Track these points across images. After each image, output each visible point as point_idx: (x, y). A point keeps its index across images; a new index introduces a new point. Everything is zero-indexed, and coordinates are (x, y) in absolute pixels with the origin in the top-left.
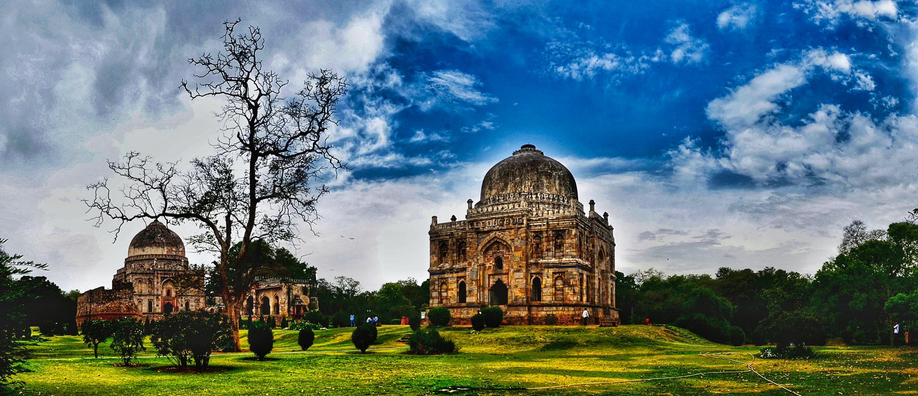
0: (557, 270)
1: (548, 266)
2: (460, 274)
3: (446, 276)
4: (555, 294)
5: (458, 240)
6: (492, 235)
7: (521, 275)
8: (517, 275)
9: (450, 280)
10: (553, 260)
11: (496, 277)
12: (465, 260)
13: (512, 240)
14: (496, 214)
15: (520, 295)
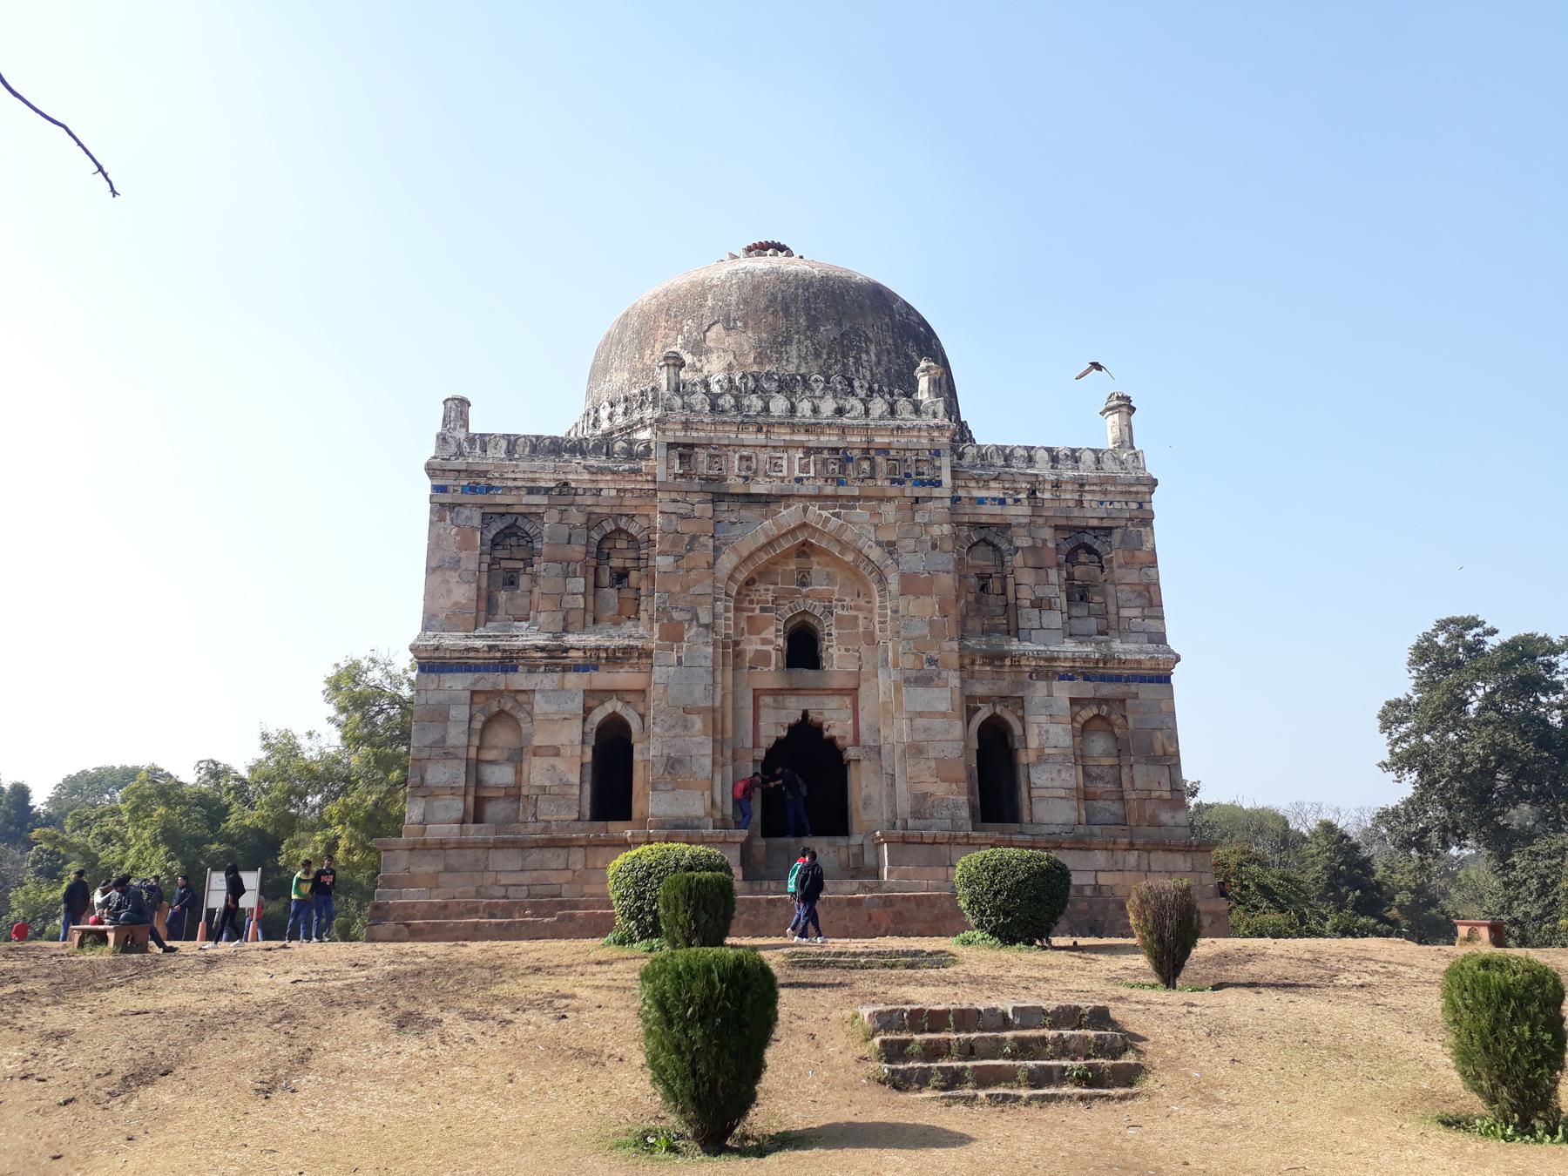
0: (1087, 689)
1: (1048, 670)
3: (520, 680)
5: (593, 521)
6: (789, 515)
9: (541, 705)
10: (1070, 647)
13: (890, 547)
15: (939, 789)
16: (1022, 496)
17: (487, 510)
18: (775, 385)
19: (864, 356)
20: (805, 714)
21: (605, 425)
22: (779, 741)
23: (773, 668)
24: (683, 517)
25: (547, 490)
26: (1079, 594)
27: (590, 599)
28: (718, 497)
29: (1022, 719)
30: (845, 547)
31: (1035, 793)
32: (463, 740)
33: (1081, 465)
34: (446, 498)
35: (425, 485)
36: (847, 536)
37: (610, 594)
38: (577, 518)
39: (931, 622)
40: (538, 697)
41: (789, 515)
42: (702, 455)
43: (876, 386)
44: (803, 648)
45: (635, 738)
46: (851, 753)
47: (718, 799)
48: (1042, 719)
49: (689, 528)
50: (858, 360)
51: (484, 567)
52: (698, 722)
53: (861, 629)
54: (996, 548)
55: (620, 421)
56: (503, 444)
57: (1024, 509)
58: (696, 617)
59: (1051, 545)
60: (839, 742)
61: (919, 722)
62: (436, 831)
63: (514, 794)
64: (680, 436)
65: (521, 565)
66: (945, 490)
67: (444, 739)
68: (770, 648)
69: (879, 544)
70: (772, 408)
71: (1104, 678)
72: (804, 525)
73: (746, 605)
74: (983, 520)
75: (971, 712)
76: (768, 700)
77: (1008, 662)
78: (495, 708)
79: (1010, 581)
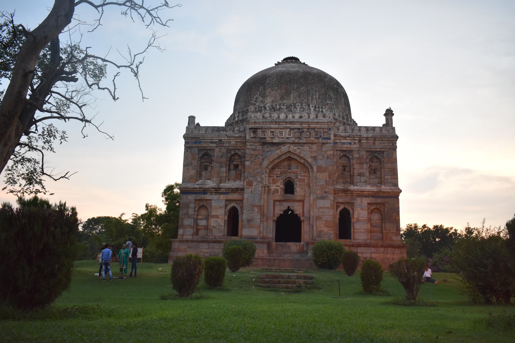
1: (362, 194)
2: (231, 196)
3: (208, 197)
4: (371, 232)
5: (228, 151)
6: (284, 149)
7: (327, 203)
8: (321, 203)
9: (214, 204)
10: (369, 188)
12: (238, 177)
14: (291, 123)
15: (326, 229)
16: (357, 142)
17: (200, 148)
18: (285, 107)
19: (314, 97)
20: (289, 207)
21: (236, 119)
22: (281, 215)
23: (279, 194)
24: (254, 150)
25: (216, 142)
26: (373, 171)
27: (227, 174)
28: (264, 144)
29: (353, 209)
30: (301, 158)
31: (355, 231)
32: (193, 213)
33: (375, 132)
34: (188, 145)
35: (183, 141)
36: (301, 155)
37: (233, 172)
38: (224, 150)
39: (326, 181)
40: (213, 201)
41: (284, 149)
42: (259, 132)
43: (317, 106)
44: (289, 187)
45: (239, 214)
46: (302, 218)
47: (262, 230)
48: (359, 209)
49: (256, 153)
50: (312, 98)
51: (199, 165)
52: (256, 209)
53: (306, 182)
54: (348, 158)
55: (240, 118)
56: (204, 129)
57: (357, 146)
58: (256, 179)
59: (365, 157)
60: (299, 215)
61: (320, 210)
62: (186, 238)
63: (207, 228)
64: (253, 126)
65: (208, 164)
66: (331, 141)
67: (188, 212)
68: (278, 188)
69: (311, 157)
70: (280, 117)
71: (378, 197)
72: (289, 152)
73: (272, 175)
74: (344, 149)
75: (337, 207)
76: (278, 203)
77: (349, 192)
78: (201, 204)
79: (352, 167)
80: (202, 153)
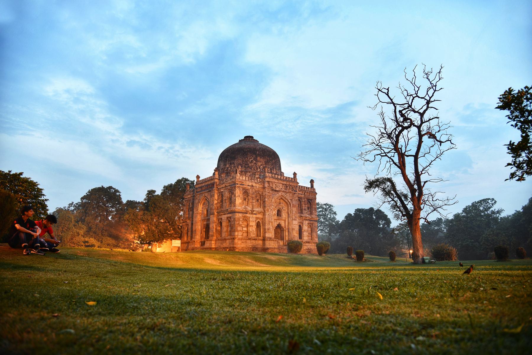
3: (248, 215)
6: (280, 194)
9: (251, 219)
11: (278, 221)
13: (291, 200)
15: (296, 235)
38: (254, 191)
44: (279, 213)
57: (303, 196)
80: (244, 190)
